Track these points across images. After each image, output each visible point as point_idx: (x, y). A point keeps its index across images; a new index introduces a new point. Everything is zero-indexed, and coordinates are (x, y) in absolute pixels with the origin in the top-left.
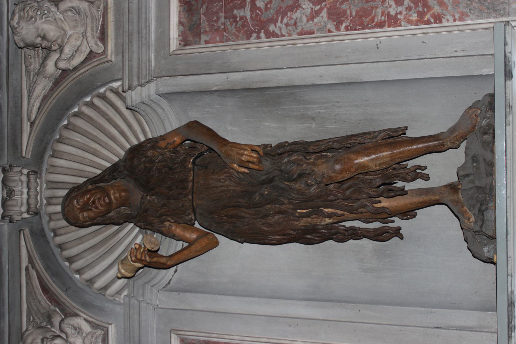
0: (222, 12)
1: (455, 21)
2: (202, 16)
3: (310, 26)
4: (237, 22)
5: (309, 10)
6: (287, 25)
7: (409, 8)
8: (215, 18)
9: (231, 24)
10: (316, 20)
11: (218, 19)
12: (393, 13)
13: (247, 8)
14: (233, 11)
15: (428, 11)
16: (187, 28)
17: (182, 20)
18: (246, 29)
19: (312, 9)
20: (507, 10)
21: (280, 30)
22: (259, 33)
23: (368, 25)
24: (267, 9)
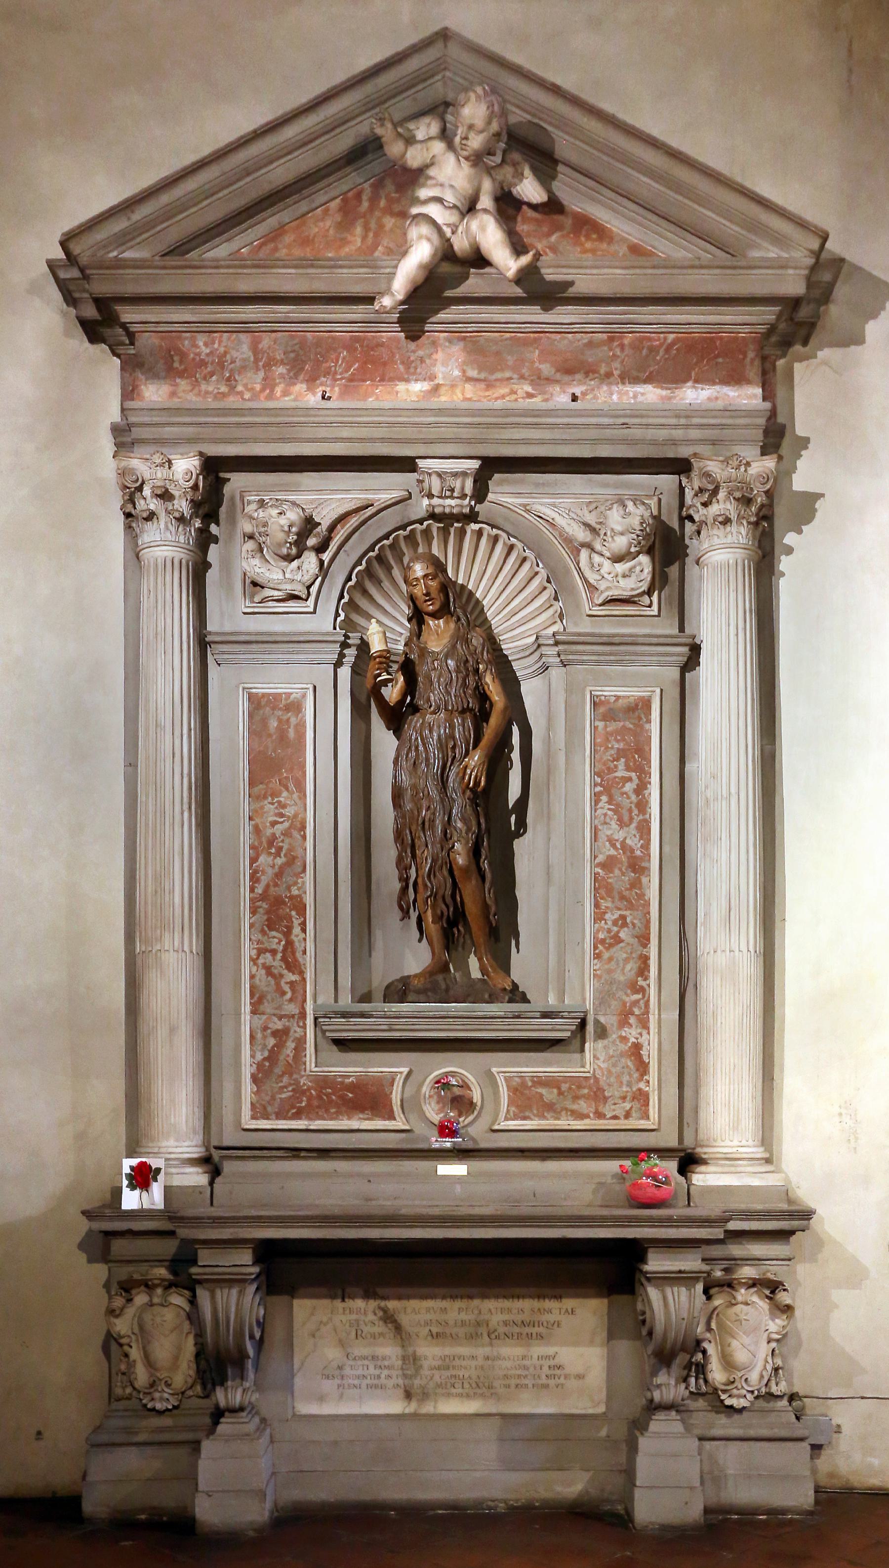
3: (602, 837)
5: (616, 838)
6: (605, 815)
7: (609, 931)
8: (619, 738)
9: (611, 755)
11: (618, 741)
12: (607, 916)
15: (605, 948)
16: (612, 706)
19: (617, 840)
21: (601, 808)
24: (622, 794)
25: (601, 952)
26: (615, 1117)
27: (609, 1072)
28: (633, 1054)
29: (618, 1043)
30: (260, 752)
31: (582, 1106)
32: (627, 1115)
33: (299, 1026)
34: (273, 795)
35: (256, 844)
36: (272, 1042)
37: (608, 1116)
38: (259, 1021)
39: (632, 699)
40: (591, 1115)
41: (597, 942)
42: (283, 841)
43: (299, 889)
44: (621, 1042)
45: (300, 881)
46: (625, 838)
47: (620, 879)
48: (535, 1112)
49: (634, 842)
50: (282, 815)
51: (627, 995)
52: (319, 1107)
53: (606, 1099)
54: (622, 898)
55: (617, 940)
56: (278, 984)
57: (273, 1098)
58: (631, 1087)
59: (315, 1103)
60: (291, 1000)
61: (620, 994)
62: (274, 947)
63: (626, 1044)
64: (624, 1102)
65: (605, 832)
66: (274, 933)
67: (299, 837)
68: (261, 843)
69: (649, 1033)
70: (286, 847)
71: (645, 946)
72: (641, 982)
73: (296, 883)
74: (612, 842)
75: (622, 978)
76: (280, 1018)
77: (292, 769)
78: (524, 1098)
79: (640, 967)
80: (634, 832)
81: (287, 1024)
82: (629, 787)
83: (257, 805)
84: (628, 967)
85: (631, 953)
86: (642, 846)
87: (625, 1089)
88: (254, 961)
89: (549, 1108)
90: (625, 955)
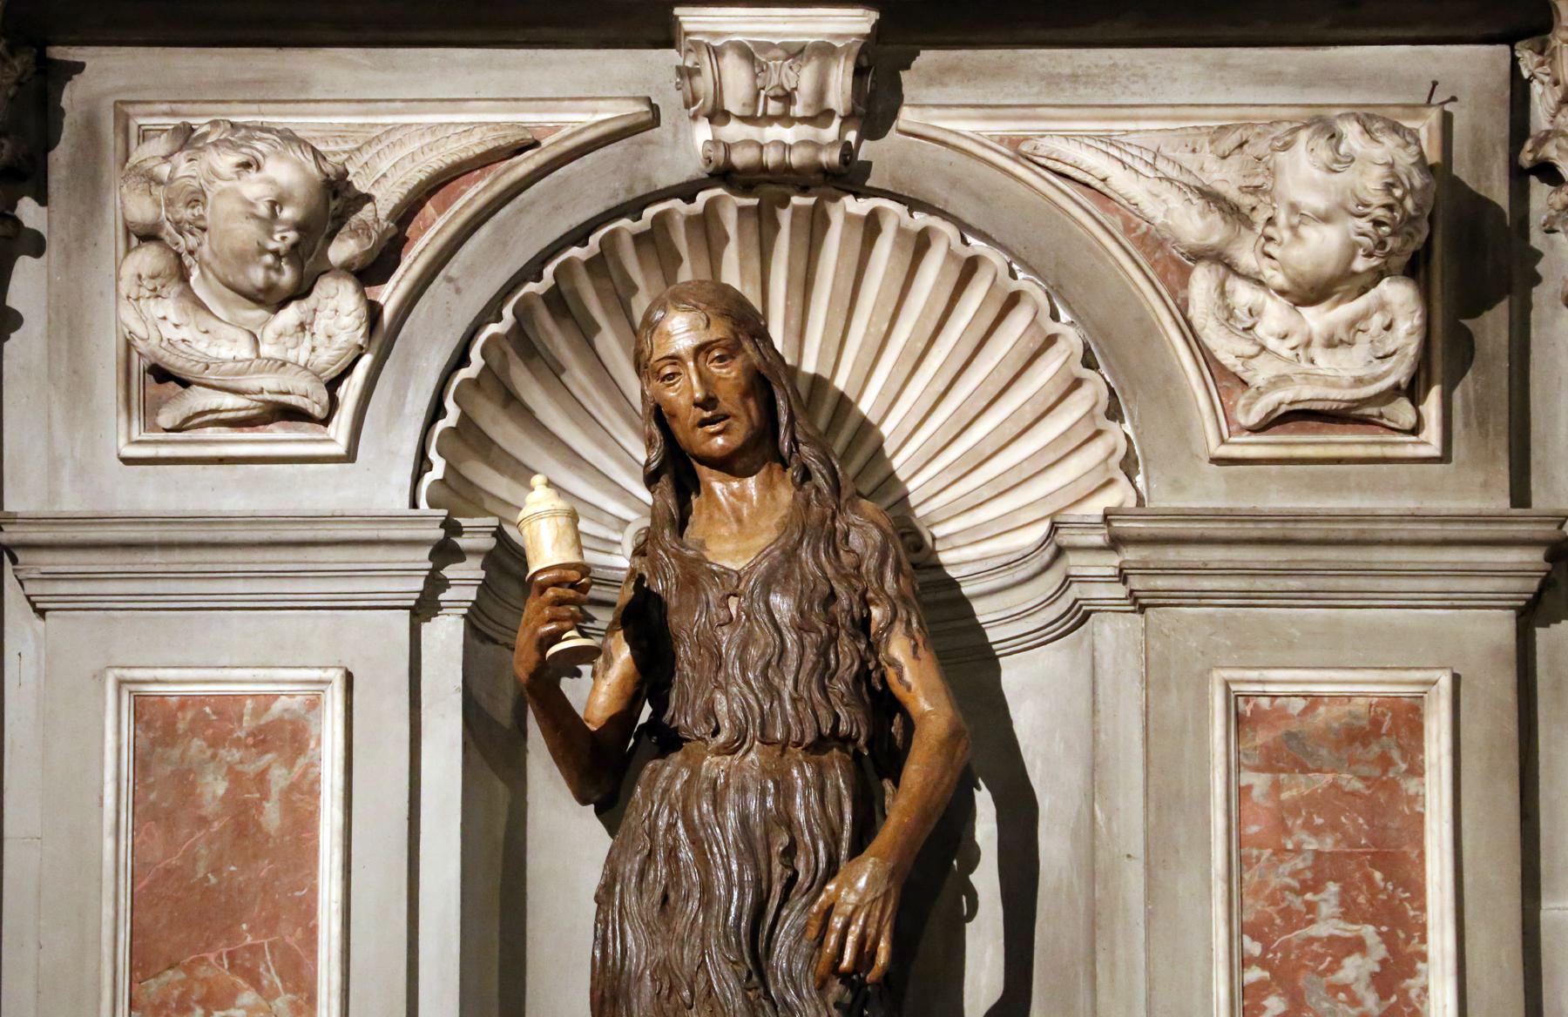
0: (1337, 843)
2: (1329, 777)
4: (1299, 893)
8: (1319, 821)
11: (1316, 831)
13: (1342, 925)
16: (1295, 727)
17: (1322, 709)
18: (1278, 921)
24: (1334, 989)
30: (168, 872)
77: (272, 923)
82: (1353, 969)
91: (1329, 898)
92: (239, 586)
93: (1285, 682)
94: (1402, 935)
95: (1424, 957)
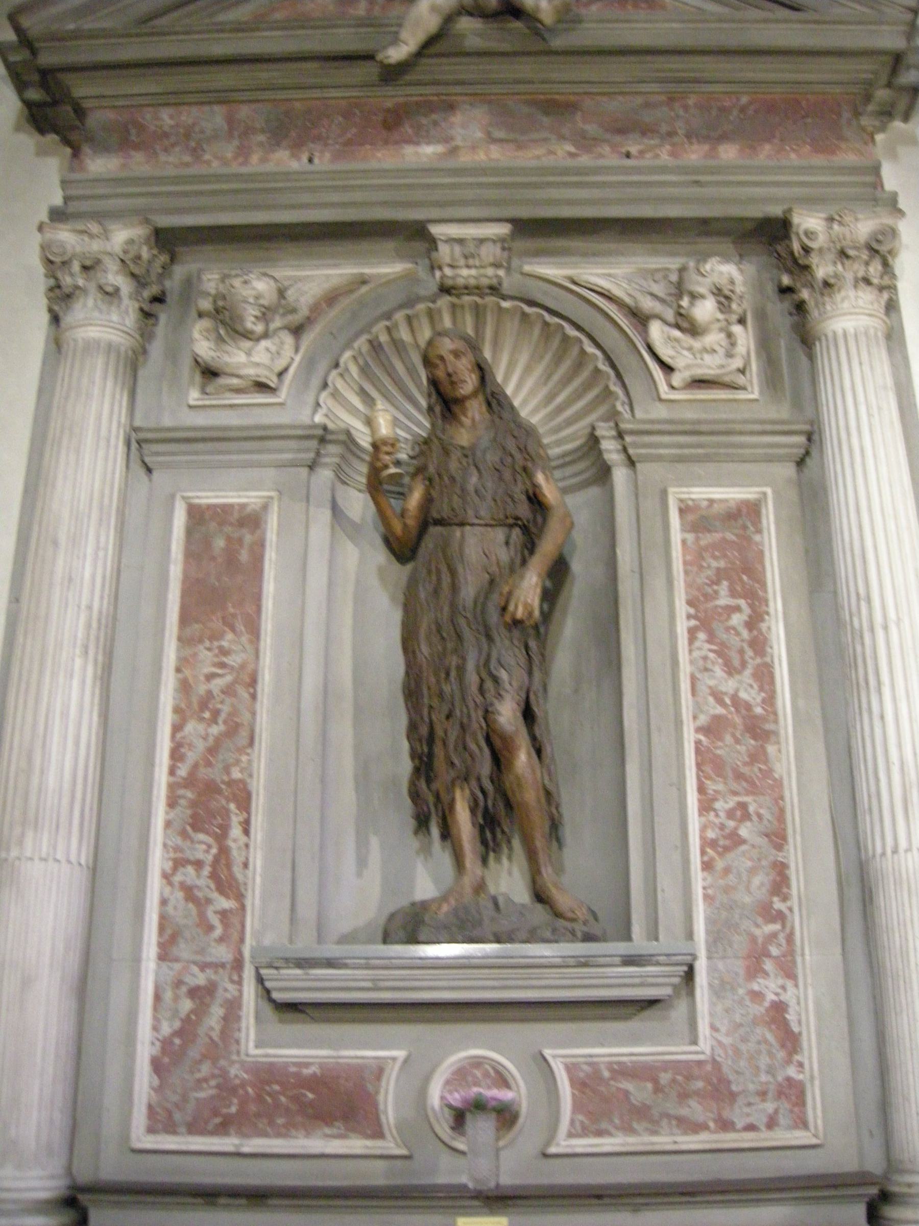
1: (704, 888)
3: (703, 689)
5: (724, 689)
6: (705, 658)
7: (722, 827)
8: (717, 553)
9: (707, 578)
10: (711, 699)
11: (715, 558)
12: (718, 805)
14: (726, 579)
16: (704, 513)
17: (715, 505)
19: (726, 694)
20: (716, 955)
21: (700, 649)
22: (695, 617)
23: (702, 771)
24: (728, 629)
25: (712, 860)
26: (751, 1128)
27: (737, 1052)
28: (773, 1021)
29: (748, 1003)
31: (695, 1110)
32: (772, 1123)
33: (232, 981)
34: (212, 638)
35: (183, 706)
36: (187, 1005)
37: (740, 1124)
38: (170, 971)
39: (732, 504)
40: (712, 1125)
41: (707, 844)
42: (222, 702)
43: (241, 772)
44: (752, 1001)
45: (244, 758)
46: (737, 690)
47: (734, 749)
48: (617, 1121)
49: (751, 695)
50: (223, 665)
51: (757, 926)
52: (258, 1115)
53: (733, 1096)
54: (739, 776)
55: (736, 840)
56: (202, 915)
57: (185, 1098)
58: (774, 1076)
59: (253, 1108)
60: (221, 940)
61: (746, 924)
62: (200, 855)
63: (760, 1005)
64: (764, 1101)
65: (708, 681)
66: (201, 836)
67: (246, 696)
68: (189, 705)
69: (796, 986)
70: (225, 709)
71: (779, 847)
72: (778, 905)
73: (238, 762)
74: (718, 697)
75: (747, 899)
76: (203, 967)
78: (600, 1099)
79: (774, 881)
80: (751, 681)
81: (213, 977)
82: (737, 620)
83: (188, 652)
84: (757, 881)
85: (759, 860)
86: (764, 701)
87: (764, 1078)
88: (166, 876)
89: (640, 1115)
90: (749, 864)
91: (723, 588)
92: (234, 457)
93: (699, 493)
94: (757, 603)
95: (768, 613)
